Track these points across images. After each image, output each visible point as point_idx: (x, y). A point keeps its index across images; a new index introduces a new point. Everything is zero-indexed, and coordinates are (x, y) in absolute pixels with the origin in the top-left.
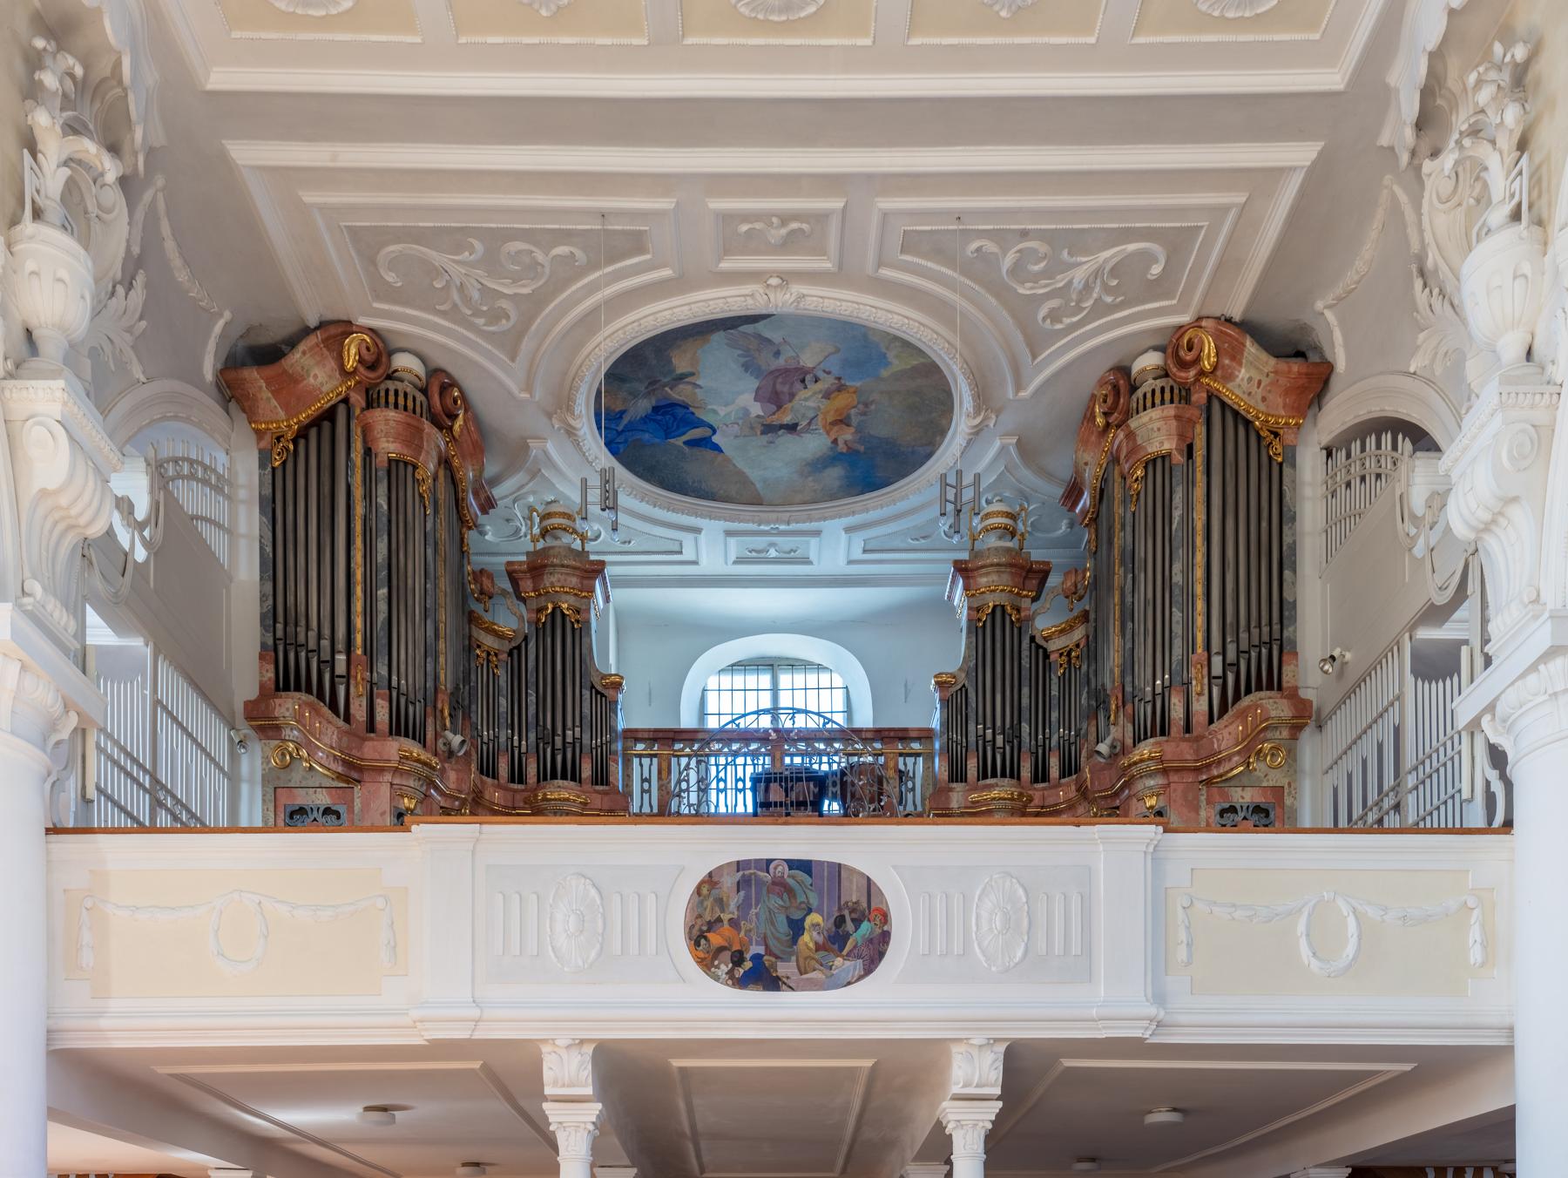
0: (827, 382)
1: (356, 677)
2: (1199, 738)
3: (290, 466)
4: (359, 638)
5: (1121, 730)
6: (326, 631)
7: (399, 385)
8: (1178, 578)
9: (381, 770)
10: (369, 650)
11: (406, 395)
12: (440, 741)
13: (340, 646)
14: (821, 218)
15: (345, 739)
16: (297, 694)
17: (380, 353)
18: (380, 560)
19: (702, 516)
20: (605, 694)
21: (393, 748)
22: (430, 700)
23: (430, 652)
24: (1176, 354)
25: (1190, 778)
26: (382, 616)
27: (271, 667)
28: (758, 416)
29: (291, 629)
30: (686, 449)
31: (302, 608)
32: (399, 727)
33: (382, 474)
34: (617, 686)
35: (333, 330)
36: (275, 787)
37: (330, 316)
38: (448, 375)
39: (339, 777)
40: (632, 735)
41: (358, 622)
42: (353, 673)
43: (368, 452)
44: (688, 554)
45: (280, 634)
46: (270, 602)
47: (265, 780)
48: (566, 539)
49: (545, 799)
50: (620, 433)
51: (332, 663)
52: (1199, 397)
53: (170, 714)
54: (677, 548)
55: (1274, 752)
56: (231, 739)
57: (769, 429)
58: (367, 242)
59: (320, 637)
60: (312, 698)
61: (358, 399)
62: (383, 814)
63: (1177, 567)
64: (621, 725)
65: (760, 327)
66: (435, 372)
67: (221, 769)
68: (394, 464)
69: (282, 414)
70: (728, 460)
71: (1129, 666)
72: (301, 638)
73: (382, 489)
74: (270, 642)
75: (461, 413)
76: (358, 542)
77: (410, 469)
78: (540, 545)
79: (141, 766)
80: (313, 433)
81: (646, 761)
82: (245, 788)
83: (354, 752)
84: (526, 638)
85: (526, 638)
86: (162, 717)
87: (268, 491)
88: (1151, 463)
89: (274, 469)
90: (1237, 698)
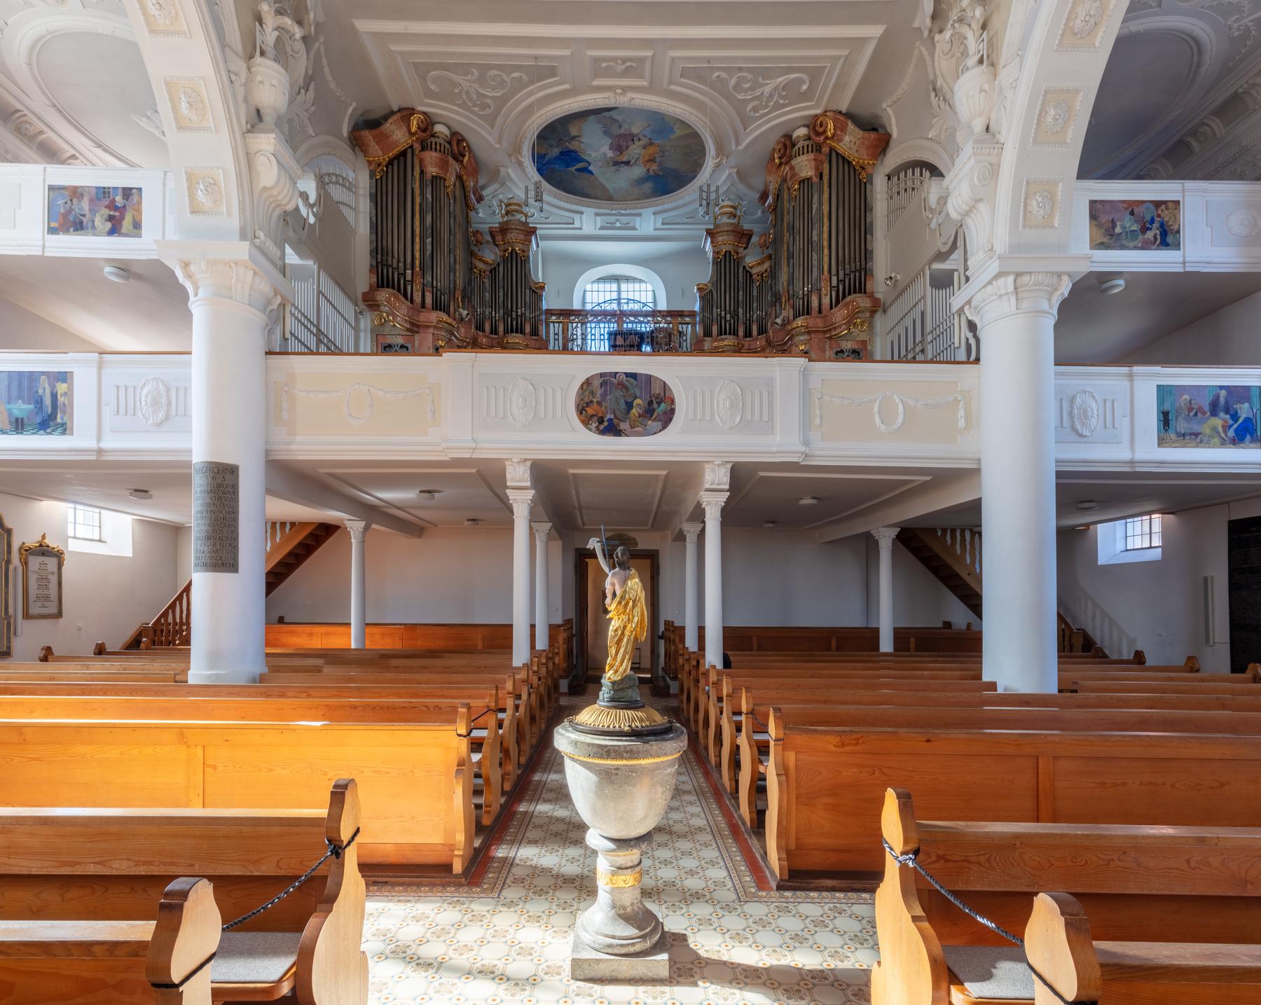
0: (644, 141)
3: (384, 178)
4: (417, 263)
6: (402, 259)
7: (437, 140)
8: (815, 238)
9: (428, 327)
10: (422, 269)
11: (440, 145)
12: (457, 313)
13: (409, 266)
14: (641, 60)
15: (411, 312)
16: (388, 290)
17: (428, 124)
19: (584, 206)
20: (537, 291)
21: (435, 316)
22: (452, 292)
23: (452, 270)
26: (429, 252)
27: (375, 276)
28: (611, 157)
29: (385, 258)
30: (576, 173)
31: (390, 248)
32: (437, 306)
34: (543, 288)
35: (405, 113)
36: (377, 334)
37: (404, 105)
38: (461, 135)
39: (408, 330)
40: (550, 312)
41: (417, 255)
43: (422, 172)
44: (577, 224)
45: (379, 260)
46: (375, 244)
47: (372, 330)
48: (518, 216)
49: (507, 342)
50: (544, 165)
51: (405, 274)
52: (825, 150)
53: (326, 298)
54: (572, 221)
56: (355, 311)
57: (616, 163)
58: (422, 70)
60: (395, 292)
61: (417, 146)
62: (429, 348)
63: (815, 232)
64: (545, 307)
65: (612, 113)
66: (454, 134)
67: (351, 325)
68: (435, 178)
70: (596, 178)
72: (390, 262)
73: (429, 190)
74: (375, 264)
75: (467, 154)
77: (442, 181)
78: (505, 219)
79: (312, 323)
80: (396, 162)
81: (556, 325)
82: (362, 335)
83: (415, 318)
84: (498, 264)
85: (498, 264)
86: (322, 299)
87: (374, 190)
88: (802, 182)
89: (376, 180)
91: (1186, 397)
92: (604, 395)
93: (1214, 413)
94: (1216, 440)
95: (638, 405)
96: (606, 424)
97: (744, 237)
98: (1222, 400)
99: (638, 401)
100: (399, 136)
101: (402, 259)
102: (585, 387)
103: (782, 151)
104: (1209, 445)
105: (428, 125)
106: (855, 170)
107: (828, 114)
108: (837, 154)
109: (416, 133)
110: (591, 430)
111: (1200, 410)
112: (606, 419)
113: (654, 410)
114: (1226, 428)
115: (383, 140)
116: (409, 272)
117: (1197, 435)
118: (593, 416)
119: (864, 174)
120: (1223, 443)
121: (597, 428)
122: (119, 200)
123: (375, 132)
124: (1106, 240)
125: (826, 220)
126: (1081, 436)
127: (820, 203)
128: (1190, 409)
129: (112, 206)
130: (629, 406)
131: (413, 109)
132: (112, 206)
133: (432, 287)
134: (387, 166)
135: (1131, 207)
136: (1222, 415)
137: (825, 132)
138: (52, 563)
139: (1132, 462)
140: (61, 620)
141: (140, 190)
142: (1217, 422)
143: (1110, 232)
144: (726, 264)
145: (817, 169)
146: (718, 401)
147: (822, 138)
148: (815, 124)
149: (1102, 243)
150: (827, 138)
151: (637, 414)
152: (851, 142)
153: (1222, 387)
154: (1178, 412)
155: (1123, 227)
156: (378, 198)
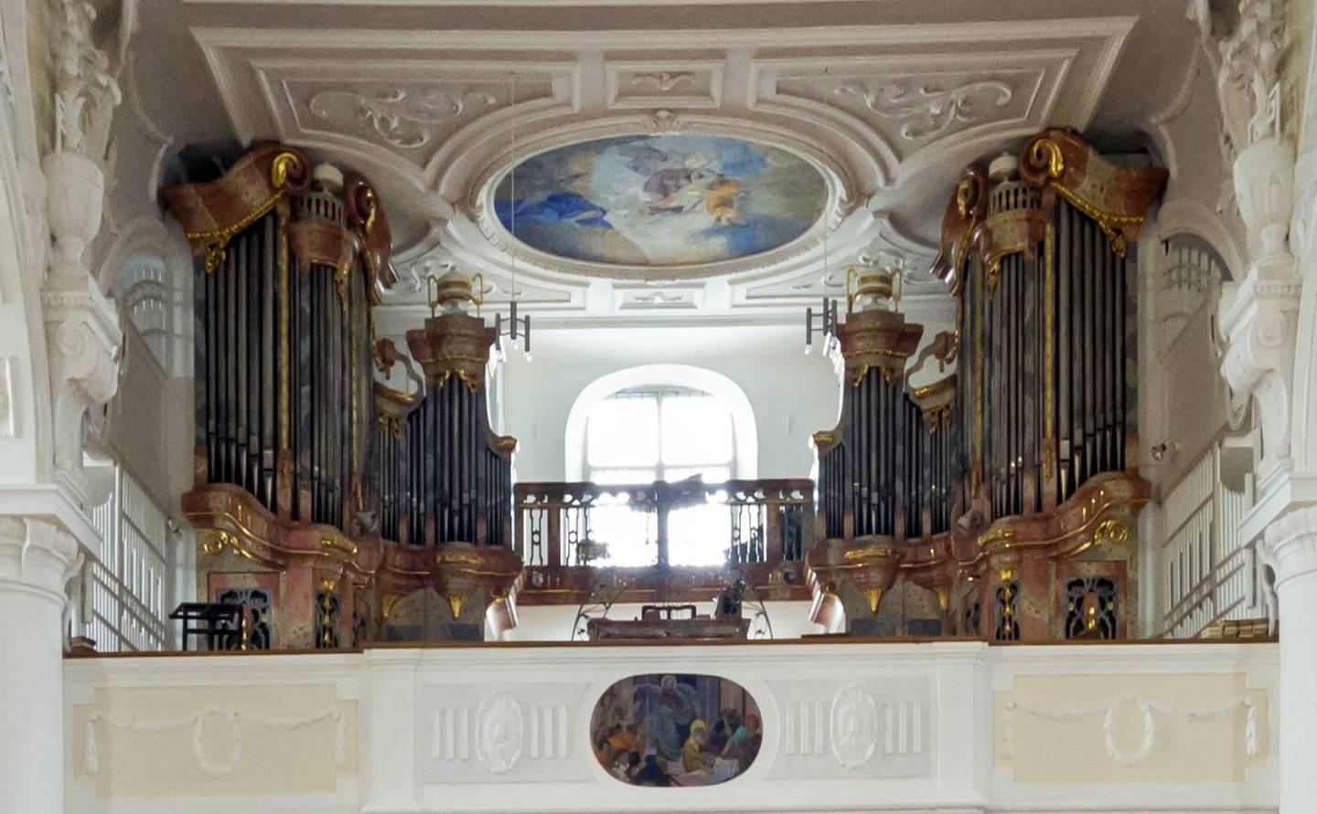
1: (282, 472)
4: (284, 434)
6: (255, 428)
11: (326, 203)
13: (268, 440)
16: (227, 486)
18: (303, 360)
26: (305, 412)
27: (204, 461)
29: (222, 425)
39: (266, 563)
41: (284, 419)
42: (279, 466)
45: (212, 428)
46: (204, 400)
47: (199, 568)
51: (260, 457)
59: (249, 433)
60: (242, 490)
61: (284, 210)
67: (160, 557)
68: (316, 268)
69: (216, 226)
72: (232, 433)
73: (305, 294)
74: (204, 436)
80: (244, 240)
82: (179, 573)
89: (207, 276)
92: (640, 715)
95: (699, 730)
96: (643, 764)
99: (698, 724)
100: (251, 195)
101: (255, 428)
102: (607, 701)
103: (970, 194)
105: (304, 171)
106: (1104, 236)
107: (1052, 134)
108: (1071, 208)
109: (283, 186)
110: (617, 777)
112: (643, 757)
113: (725, 738)
115: (224, 204)
116: (269, 453)
118: (620, 752)
119: (1120, 243)
121: (628, 772)
123: (208, 188)
130: (684, 733)
131: (277, 143)
133: (312, 477)
134: (227, 249)
137: (1047, 166)
146: (835, 720)
147: (1041, 179)
150: (1050, 178)
151: (696, 747)
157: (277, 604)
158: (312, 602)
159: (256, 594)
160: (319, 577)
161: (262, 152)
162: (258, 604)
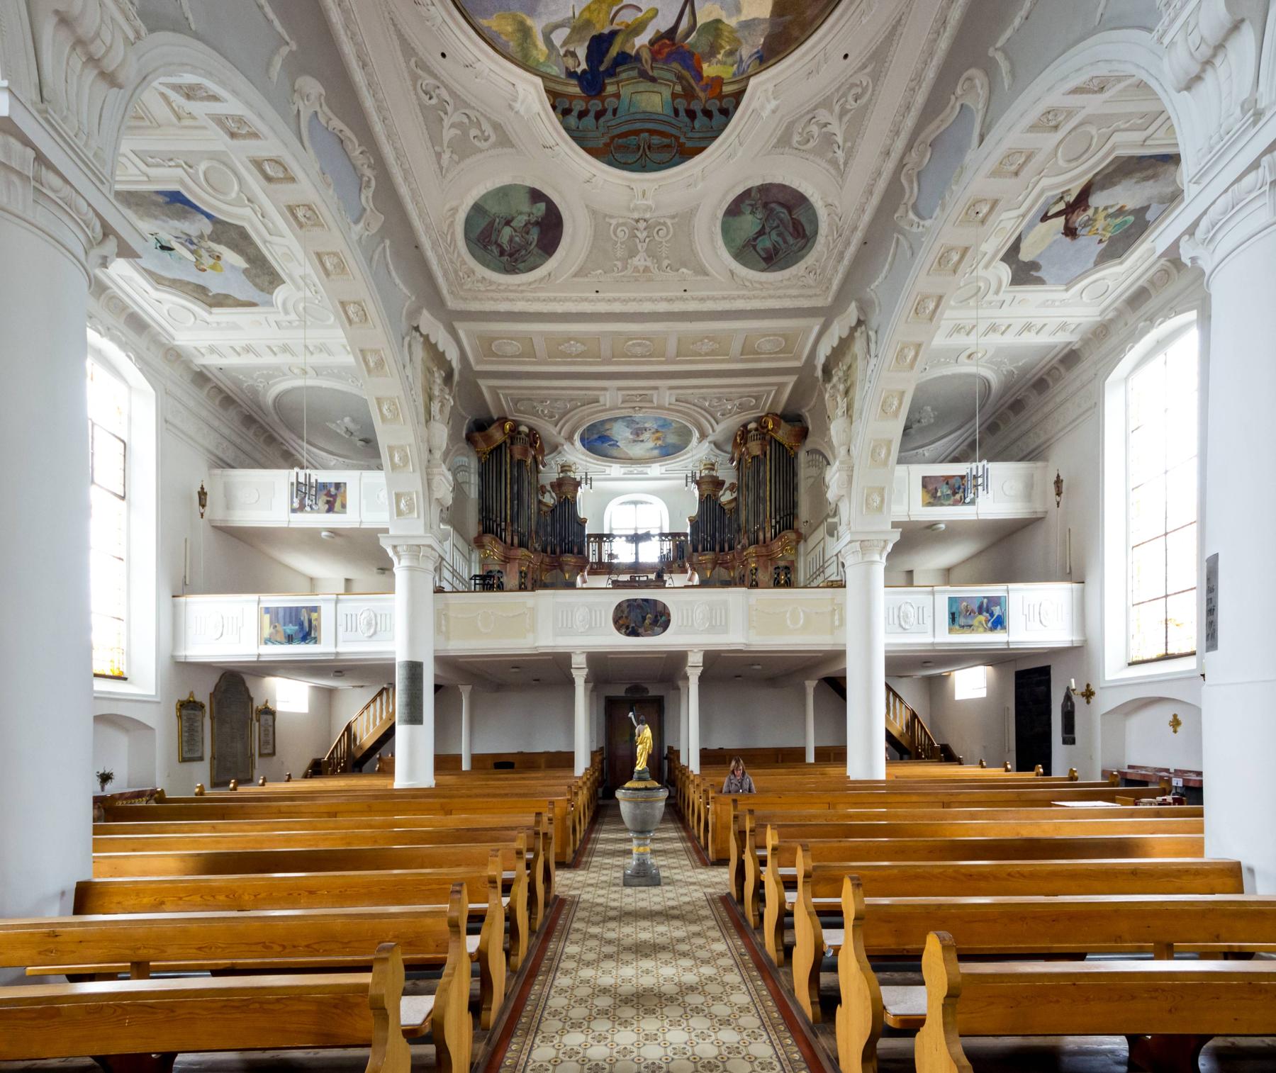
2: (768, 546)
4: (509, 517)
5: (745, 541)
6: (499, 515)
8: (762, 495)
9: (515, 559)
13: (503, 520)
22: (530, 534)
24: (760, 424)
25: (765, 558)
26: (516, 510)
32: (521, 545)
33: (516, 465)
41: (509, 512)
43: (511, 456)
47: (480, 563)
52: (768, 437)
55: (791, 549)
59: (497, 517)
61: (508, 441)
63: (761, 491)
69: (485, 446)
71: (747, 520)
73: (516, 470)
76: (509, 486)
82: (473, 564)
88: (753, 458)
90: (780, 532)
91: (965, 604)
93: (980, 613)
94: (981, 629)
97: (718, 484)
98: (985, 605)
104: (977, 632)
106: (787, 450)
108: (776, 440)
111: (973, 611)
114: (987, 621)
115: (488, 439)
116: (503, 524)
117: (970, 626)
119: (792, 452)
120: (985, 630)
122: (333, 490)
123: (483, 434)
124: (931, 500)
125: (768, 483)
126: (904, 629)
127: (765, 472)
128: (967, 611)
129: (329, 494)
131: (506, 418)
132: (329, 494)
135: (947, 480)
136: (985, 614)
137: (767, 426)
138: (270, 718)
139: (933, 644)
140: (275, 758)
141: (345, 484)
142: (982, 618)
143: (934, 496)
144: (709, 503)
145: (762, 450)
147: (765, 431)
148: (758, 420)
149: (930, 503)
150: (768, 430)
152: (783, 434)
153: (984, 597)
154: (960, 613)
155: (942, 492)
156: (483, 475)
157: (506, 575)
158: (518, 574)
159: (499, 572)
160: (521, 566)
161: (502, 421)
162: (499, 575)
